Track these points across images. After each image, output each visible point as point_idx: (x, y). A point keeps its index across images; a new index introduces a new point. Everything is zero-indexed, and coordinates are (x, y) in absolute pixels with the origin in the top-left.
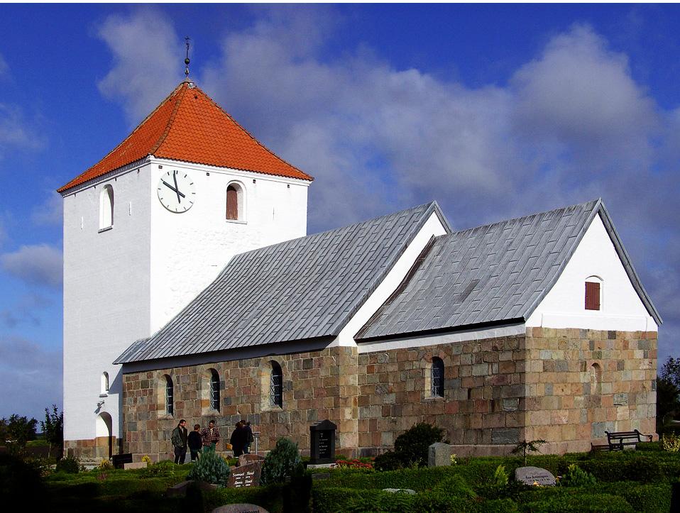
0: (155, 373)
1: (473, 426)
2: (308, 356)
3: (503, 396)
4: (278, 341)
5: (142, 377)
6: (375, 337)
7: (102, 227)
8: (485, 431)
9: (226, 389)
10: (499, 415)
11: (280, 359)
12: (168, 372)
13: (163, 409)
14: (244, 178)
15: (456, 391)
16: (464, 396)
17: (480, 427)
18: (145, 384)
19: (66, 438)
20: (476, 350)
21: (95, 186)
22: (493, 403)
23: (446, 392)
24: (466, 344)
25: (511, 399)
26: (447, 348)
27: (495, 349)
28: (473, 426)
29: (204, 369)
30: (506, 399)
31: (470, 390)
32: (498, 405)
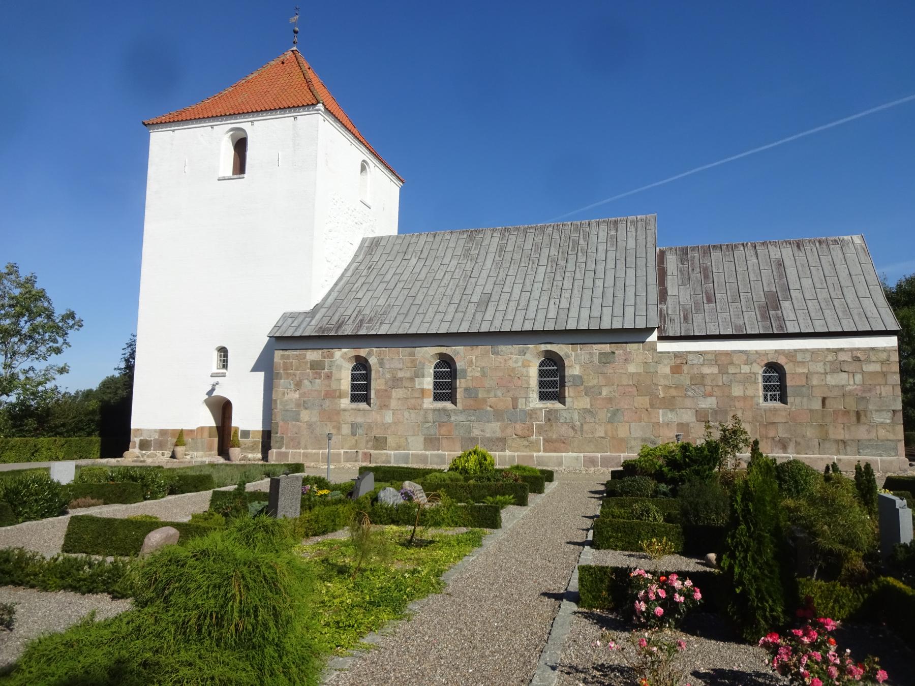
0: (338, 354)
1: (832, 436)
2: (607, 348)
3: (870, 407)
4: (346, 334)
5: (312, 355)
6: (851, 332)
7: (221, 175)
8: (849, 443)
9: (468, 378)
10: (866, 427)
11: (559, 349)
12: (363, 352)
13: (346, 397)
14: (245, 124)
15: (805, 399)
16: (817, 405)
17: (842, 437)
18: (316, 366)
19: (135, 424)
20: (830, 358)
21: (212, 127)
22: (858, 414)
23: (789, 400)
24: (814, 352)
25: (882, 410)
26: (791, 355)
27: (857, 359)
28: (832, 436)
29: (428, 354)
30: (877, 411)
31: (824, 400)
32: (865, 416)
